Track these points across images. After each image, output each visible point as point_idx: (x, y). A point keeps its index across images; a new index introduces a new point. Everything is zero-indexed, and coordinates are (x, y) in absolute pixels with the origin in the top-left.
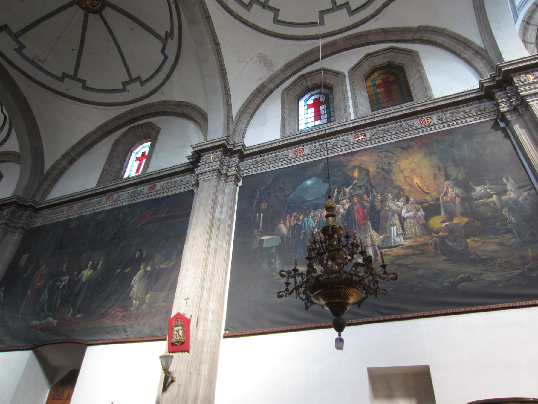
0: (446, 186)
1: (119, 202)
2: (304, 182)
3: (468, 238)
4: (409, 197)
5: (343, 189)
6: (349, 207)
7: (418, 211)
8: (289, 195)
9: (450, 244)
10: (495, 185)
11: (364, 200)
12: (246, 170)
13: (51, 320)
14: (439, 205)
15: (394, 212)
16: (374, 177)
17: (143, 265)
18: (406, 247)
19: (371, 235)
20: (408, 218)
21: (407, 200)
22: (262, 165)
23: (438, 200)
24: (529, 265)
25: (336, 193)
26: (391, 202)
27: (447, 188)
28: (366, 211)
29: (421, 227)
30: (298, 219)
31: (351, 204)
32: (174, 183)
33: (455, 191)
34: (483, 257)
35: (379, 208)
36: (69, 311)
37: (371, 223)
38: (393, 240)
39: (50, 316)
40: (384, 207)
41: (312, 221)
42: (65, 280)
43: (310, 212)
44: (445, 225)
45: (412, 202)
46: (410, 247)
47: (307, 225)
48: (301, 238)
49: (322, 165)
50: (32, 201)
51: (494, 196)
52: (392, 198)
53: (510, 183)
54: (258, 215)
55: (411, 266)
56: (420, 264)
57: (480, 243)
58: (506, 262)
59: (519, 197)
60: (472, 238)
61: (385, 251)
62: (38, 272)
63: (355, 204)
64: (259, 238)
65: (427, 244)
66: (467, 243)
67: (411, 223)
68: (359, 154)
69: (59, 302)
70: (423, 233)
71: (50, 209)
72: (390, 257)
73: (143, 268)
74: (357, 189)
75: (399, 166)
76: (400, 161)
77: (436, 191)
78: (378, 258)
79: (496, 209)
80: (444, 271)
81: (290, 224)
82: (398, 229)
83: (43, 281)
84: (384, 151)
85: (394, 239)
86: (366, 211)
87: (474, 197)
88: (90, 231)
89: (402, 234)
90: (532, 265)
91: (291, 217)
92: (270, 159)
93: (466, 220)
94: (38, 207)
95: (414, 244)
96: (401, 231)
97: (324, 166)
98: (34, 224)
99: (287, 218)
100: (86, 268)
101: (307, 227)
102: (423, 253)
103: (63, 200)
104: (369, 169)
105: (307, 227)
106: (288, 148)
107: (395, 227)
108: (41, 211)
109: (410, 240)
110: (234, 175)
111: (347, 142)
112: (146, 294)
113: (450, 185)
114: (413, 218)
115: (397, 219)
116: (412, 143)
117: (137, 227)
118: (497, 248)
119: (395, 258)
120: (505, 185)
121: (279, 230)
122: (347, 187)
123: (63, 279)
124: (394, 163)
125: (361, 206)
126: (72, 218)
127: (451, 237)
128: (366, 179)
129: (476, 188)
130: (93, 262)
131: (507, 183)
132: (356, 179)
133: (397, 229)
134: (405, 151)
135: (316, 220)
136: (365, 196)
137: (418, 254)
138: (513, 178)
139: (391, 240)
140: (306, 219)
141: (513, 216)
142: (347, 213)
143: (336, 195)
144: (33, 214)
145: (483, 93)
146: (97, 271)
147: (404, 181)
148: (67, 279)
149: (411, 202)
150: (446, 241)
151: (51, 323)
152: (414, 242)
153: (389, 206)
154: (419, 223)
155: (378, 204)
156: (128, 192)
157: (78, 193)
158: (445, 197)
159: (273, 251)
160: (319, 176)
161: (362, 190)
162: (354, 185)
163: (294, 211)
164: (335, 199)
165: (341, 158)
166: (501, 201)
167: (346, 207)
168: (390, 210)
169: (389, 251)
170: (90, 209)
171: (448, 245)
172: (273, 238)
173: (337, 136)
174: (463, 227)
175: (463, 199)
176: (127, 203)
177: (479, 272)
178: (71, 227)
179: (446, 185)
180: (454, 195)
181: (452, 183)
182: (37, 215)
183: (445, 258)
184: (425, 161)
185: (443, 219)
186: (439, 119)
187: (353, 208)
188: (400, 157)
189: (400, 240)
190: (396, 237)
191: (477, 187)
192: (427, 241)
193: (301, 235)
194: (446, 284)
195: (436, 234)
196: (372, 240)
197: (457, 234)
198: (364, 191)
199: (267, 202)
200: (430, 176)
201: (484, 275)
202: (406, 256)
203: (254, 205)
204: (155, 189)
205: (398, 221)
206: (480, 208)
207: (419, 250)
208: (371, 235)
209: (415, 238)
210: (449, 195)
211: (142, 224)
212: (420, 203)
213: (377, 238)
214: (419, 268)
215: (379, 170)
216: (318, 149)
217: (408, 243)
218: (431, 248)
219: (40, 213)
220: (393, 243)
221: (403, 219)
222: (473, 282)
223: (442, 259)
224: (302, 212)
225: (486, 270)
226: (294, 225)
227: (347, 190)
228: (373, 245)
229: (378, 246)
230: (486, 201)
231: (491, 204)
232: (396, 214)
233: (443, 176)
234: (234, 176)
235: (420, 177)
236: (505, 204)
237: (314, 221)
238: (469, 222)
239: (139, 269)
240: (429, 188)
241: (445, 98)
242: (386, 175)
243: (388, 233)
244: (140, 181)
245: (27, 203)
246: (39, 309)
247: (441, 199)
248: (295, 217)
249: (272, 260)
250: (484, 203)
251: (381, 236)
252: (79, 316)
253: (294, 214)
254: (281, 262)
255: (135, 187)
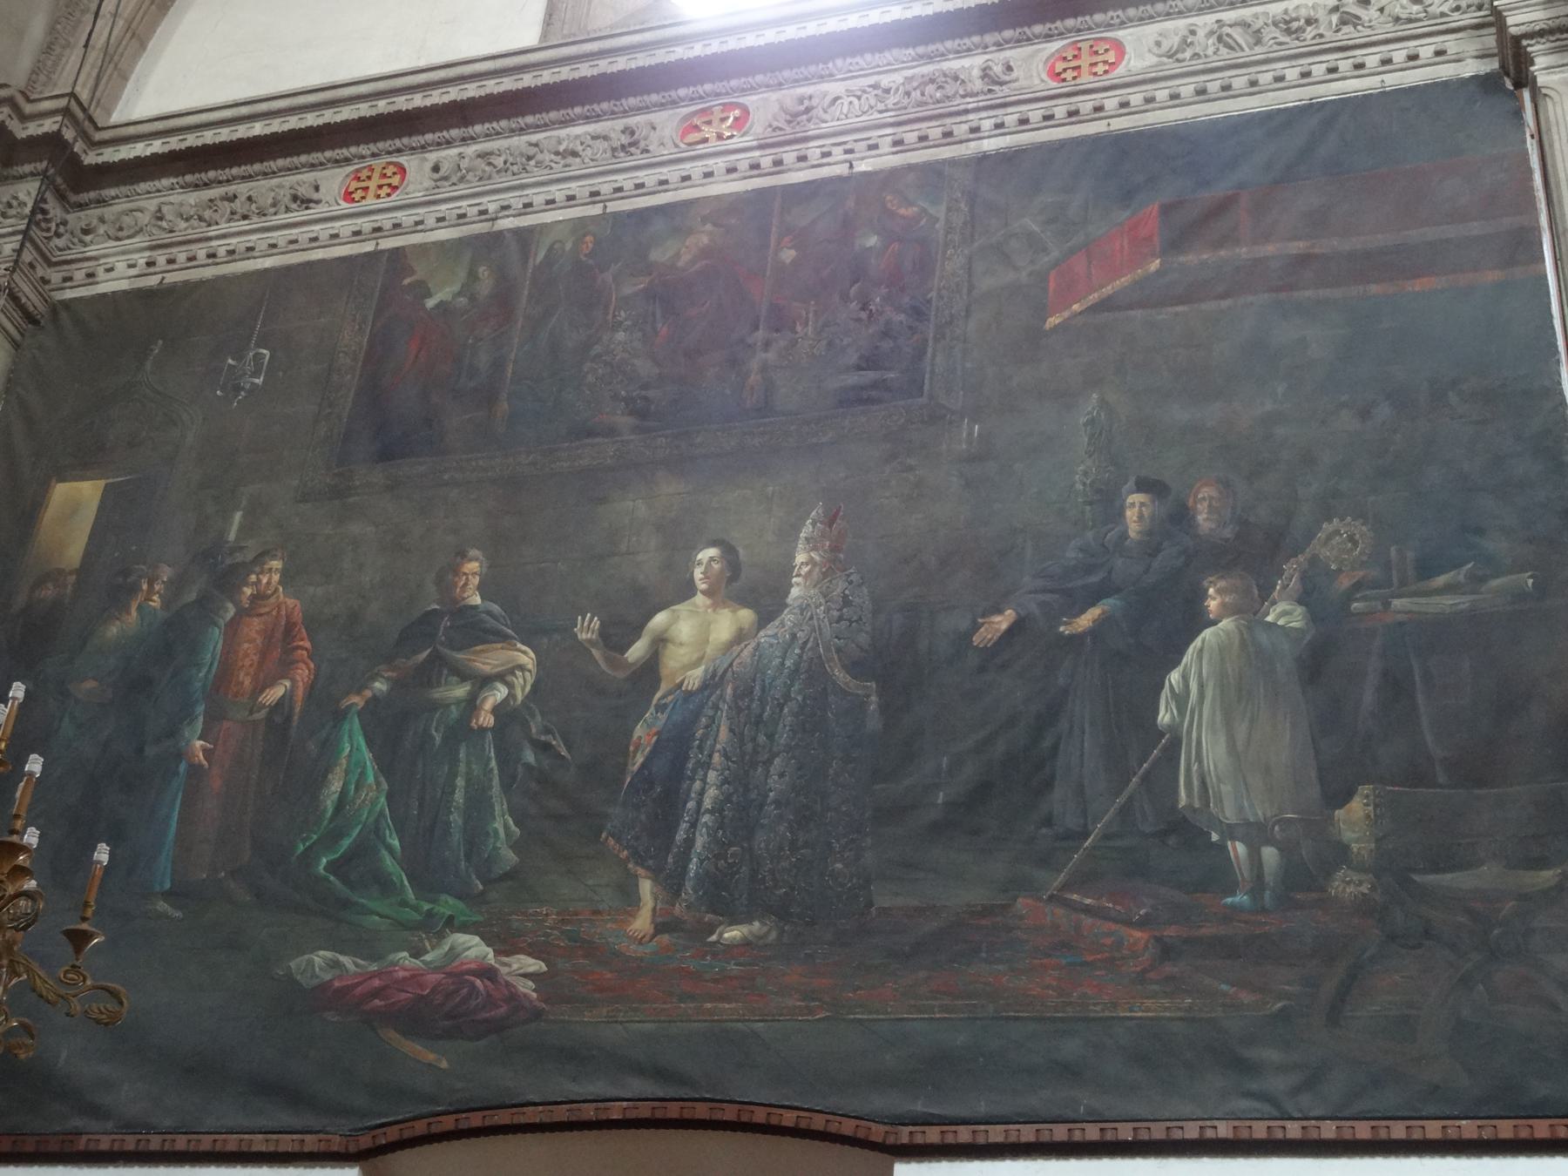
1: (813, 151)
13: (471, 953)
17: (1219, 591)
32: (1271, 33)
36: (630, 898)
39: (452, 924)
42: (512, 672)
50: (66, 112)
62: (231, 610)
69: (502, 823)
71: (189, 178)
73: (1226, 610)
83: (303, 674)
88: (621, 336)
94: (90, 159)
98: (79, 276)
100: (686, 590)
103: (312, 120)
108: (113, 192)
112: (1341, 797)
117: (1053, 321)
123: (489, 660)
126: (423, 248)
130: (729, 550)
144: (54, 209)
146: (788, 617)
148: (522, 668)
151: (488, 973)
156: (875, 86)
157: (442, 74)
170: (558, 192)
176: (889, 160)
178: (430, 303)
182: (77, 219)
204: (1121, 70)
211: (1094, 298)
219: (101, 202)
239: (1196, 621)
244: (874, 27)
245: (24, 118)
246: (333, 867)
252: (733, 934)
255: (921, 50)
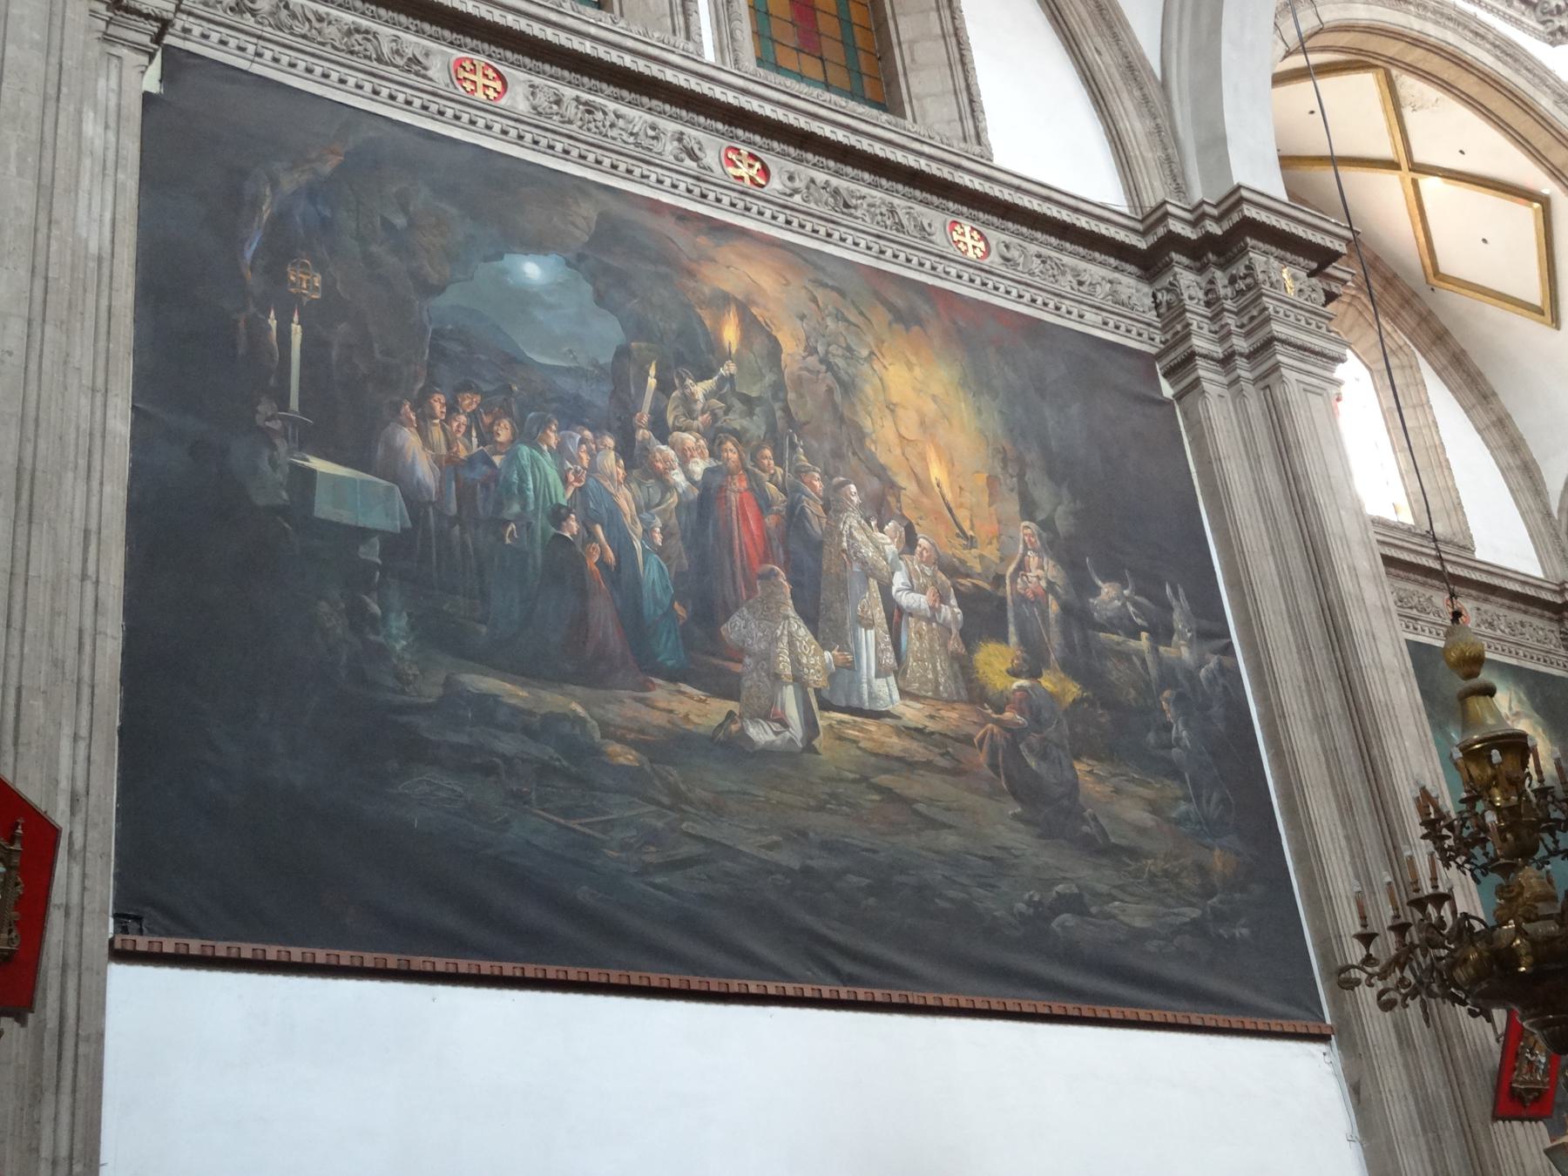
0: (1024, 540)
2: (507, 257)
3: (1077, 757)
4: (916, 527)
5: (682, 381)
6: (707, 471)
7: (943, 599)
8: (440, 290)
9: (1033, 764)
10: (1147, 597)
11: (764, 471)
12: (190, 14)
14: (1003, 601)
15: (869, 571)
16: (799, 382)
18: (908, 728)
19: (790, 635)
20: (911, 615)
21: (910, 541)
22: (268, 32)
23: (999, 580)
24: (1215, 899)
25: (652, 382)
26: (859, 523)
27: (1026, 548)
28: (770, 521)
29: (951, 666)
30: (487, 437)
31: (712, 463)
33: (1046, 568)
34: (1113, 840)
35: (820, 532)
37: (788, 580)
38: (865, 686)
40: (833, 531)
41: (553, 475)
43: (544, 424)
44: (1020, 688)
45: (924, 552)
46: (917, 732)
47: (531, 486)
48: (508, 541)
49: (586, 212)
51: (1144, 635)
52: (861, 506)
53: (1181, 608)
54: (273, 323)
55: (921, 807)
56: (948, 809)
57: (1106, 789)
58: (1166, 873)
59: (1201, 667)
60: (1090, 762)
61: (841, 722)
63: (730, 473)
64: (290, 453)
65: (967, 740)
66: (1076, 777)
67: (920, 635)
68: (741, 245)
70: (958, 693)
72: (859, 753)
74: (738, 405)
75: (881, 379)
76: (886, 363)
77: (995, 541)
78: (816, 743)
79: (1148, 684)
80: (1016, 857)
81: (449, 447)
82: (882, 645)
84: (833, 288)
85: (869, 683)
86: (770, 521)
87: (1095, 614)
89: (896, 674)
90: (1221, 902)
91: (452, 409)
92: (331, 31)
93: (1073, 690)
95: (932, 726)
96: (889, 659)
97: (598, 223)
99: (433, 408)
101: (531, 494)
102: (957, 771)
104: (780, 337)
105: (531, 494)
106: (426, 26)
107: (873, 632)
109: (921, 706)
110: (156, 19)
111: (693, 156)
113: (1033, 540)
114: (929, 621)
115: (878, 605)
116: (924, 309)
118: (1144, 818)
119: (873, 760)
120: (1171, 609)
121: (395, 453)
122: (700, 378)
124: (865, 359)
125: (751, 489)
127: (1034, 739)
128: (769, 378)
129: (1100, 583)
131: (1174, 603)
132: (729, 356)
133: (877, 644)
134: (898, 327)
135: (571, 478)
136: (768, 452)
137: (943, 770)
138: (1188, 597)
139: (861, 683)
140: (525, 450)
141: (1186, 725)
142: (701, 497)
143: (655, 398)
145: (1143, 245)
147: (898, 451)
149: (921, 553)
150: (1021, 746)
152: (932, 717)
153: (851, 535)
154: (945, 645)
155: (813, 508)
158: (1019, 580)
159: (371, 552)
160: (576, 262)
161: (755, 418)
162: (723, 379)
163: (467, 387)
164: (651, 412)
165: (668, 226)
166: (1159, 660)
167: (699, 467)
168: (855, 553)
169: (854, 726)
171: (1028, 766)
172: (363, 482)
173: (655, 103)
174: (1066, 711)
175: (1066, 609)
177: (1102, 888)
179: (1021, 534)
180: (1043, 583)
181: (1040, 536)
183: (1019, 810)
184: (963, 405)
185: (1013, 661)
186: (1007, 260)
187: (722, 489)
188: (886, 344)
189: (886, 692)
190: (877, 676)
191: (1104, 582)
192: (970, 729)
193: (506, 523)
194: (1021, 906)
195: (996, 713)
196: (796, 661)
197: (1050, 732)
198: (764, 428)
199: (320, 266)
200: (977, 472)
201: (1117, 903)
202: (907, 764)
203: (249, 254)
205: (879, 614)
206: (1109, 664)
207: (948, 753)
208: (790, 635)
209: (933, 702)
210: (1034, 573)
212: (952, 570)
213: (818, 660)
214: (945, 826)
215: (812, 361)
216: (570, 122)
217: (913, 713)
218: (982, 758)
220: (866, 697)
221: (896, 611)
222: (1090, 919)
223: (1010, 812)
224: (509, 414)
225: (1121, 888)
226: (471, 461)
227: (700, 389)
228: (799, 681)
229: (817, 691)
230: (1124, 642)
231: (1135, 659)
232: (875, 583)
233: (1015, 496)
234: (154, 27)
235: (950, 464)
236: (1169, 674)
237: (565, 481)
238: (1082, 700)
240: (974, 520)
241: (1022, 184)
242: (838, 397)
243: (848, 649)
247: (1008, 582)
248: (474, 416)
249: (368, 600)
250: (1119, 648)
251: (827, 654)
253: (470, 402)
254: (413, 628)
